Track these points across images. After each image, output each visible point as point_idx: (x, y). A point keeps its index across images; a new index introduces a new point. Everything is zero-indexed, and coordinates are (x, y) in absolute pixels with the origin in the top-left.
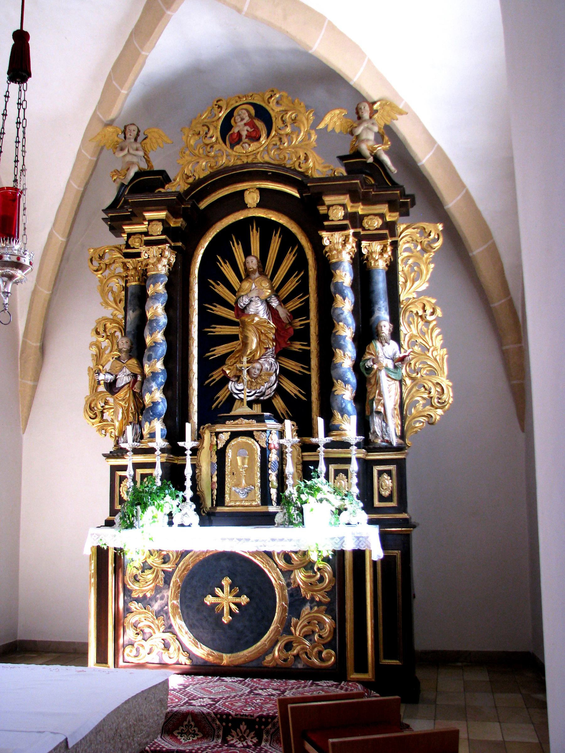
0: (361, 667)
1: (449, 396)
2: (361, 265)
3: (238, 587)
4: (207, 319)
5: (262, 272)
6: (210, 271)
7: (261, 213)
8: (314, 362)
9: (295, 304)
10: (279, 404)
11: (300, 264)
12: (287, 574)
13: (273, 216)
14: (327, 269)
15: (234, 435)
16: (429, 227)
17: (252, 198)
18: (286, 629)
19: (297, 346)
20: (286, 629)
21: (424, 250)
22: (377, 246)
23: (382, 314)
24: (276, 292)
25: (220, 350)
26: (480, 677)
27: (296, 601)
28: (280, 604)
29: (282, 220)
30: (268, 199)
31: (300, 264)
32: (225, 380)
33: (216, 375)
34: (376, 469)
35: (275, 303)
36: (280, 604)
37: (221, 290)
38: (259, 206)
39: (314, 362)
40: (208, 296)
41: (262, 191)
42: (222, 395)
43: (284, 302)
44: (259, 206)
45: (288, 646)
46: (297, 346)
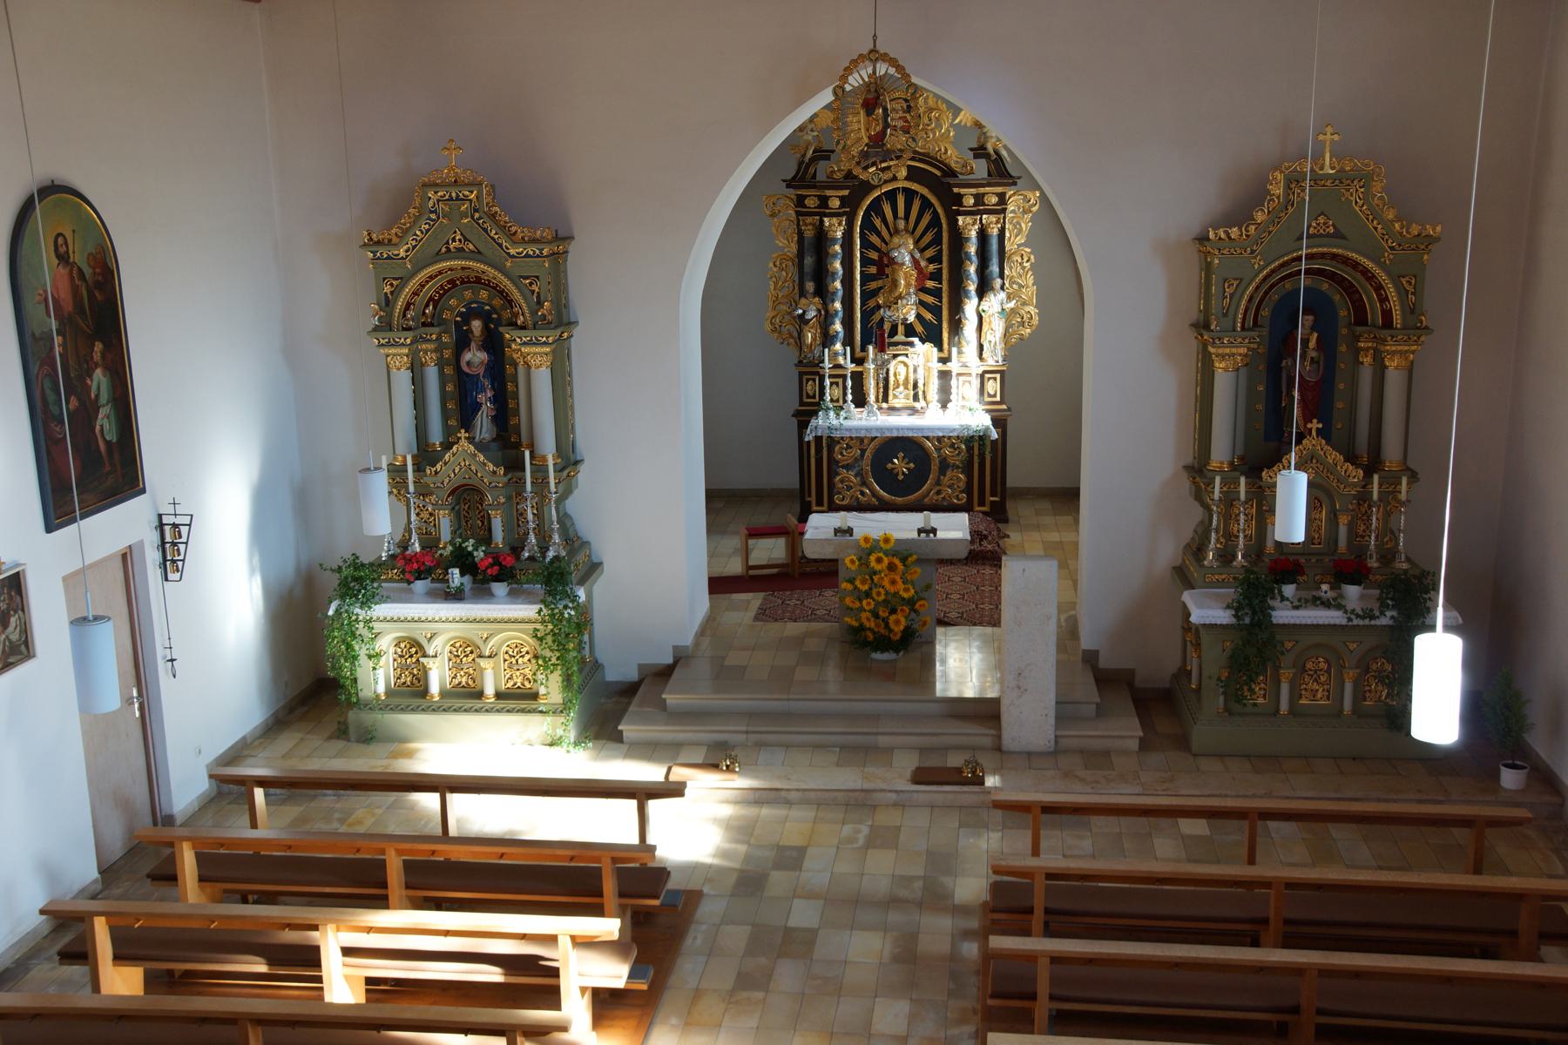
0: (982, 503)
1: (1035, 321)
2: (983, 236)
3: (909, 458)
4: (865, 261)
5: (906, 230)
6: (868, 225)
7: (907, 184)
8: (945, 300)
9: (930, 253)
10: (919, 328)
11: (935, 222)
12: (938, 449)
13: (914, 186)
14: (958, 240)
15: (895, 356)
16: (1030, 195)
17: (903, 173)
18: (938, 482)
19: (930, 284)
20: (938, 482)
21: (1025, 212)
22: (993, 218)
23: (995, 268)
24: (916, 243)
25: (874, 285)
26: (1047, 505)
27: (944, 466)
28: (935, 467)
29: (924, 191)
30: (913, 174)
31: (935, 222)
32: (879, 307)
33: (872, 303)
34: (998, 398)
35: (918, 255)
36: (935, 467)
37: (874, 239)
38: (906, 179)
39: (945, 300)
40: (866, 244)
41: (909, 167)
42: (876, 318)
43: (922, 251)
44: (906, 179)
45: (938, 493)
46: (930, 284)
